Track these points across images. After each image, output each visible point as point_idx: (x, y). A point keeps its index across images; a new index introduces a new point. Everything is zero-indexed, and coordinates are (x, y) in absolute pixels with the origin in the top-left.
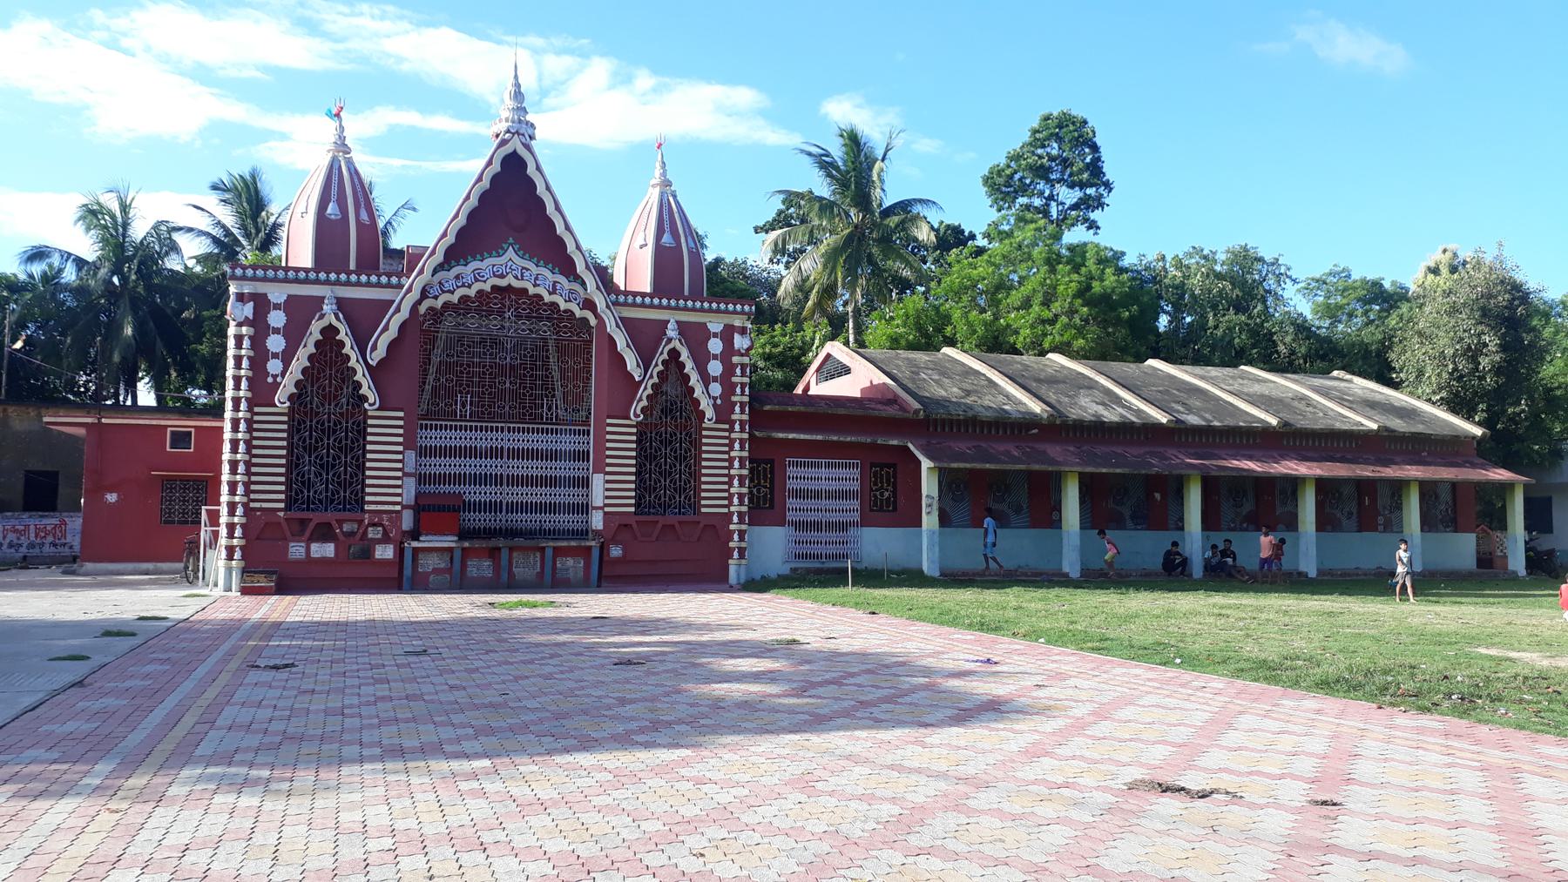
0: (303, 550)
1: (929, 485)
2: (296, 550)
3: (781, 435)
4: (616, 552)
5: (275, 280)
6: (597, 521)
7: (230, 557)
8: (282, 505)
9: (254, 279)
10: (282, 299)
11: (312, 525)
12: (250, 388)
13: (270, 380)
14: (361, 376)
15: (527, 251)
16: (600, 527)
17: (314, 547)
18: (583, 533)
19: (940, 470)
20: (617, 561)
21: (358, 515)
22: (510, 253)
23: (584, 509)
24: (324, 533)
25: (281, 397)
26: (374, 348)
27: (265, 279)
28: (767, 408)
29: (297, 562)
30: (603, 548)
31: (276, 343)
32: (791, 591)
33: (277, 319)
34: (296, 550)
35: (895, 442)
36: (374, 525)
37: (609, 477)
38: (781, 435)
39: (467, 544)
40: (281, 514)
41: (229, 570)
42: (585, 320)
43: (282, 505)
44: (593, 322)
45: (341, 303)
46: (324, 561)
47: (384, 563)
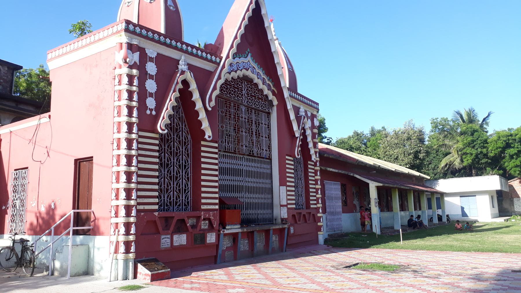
0: (169, 240)
1: (373, 194)
2: (165, 241)
3: (331, 170)
4: (292, 231)
5: (153, 40)
6: (284, 213)
7: (127, 251)
8: (156, 207)
9: (140, 35)
10: (154, 55)
11: (174, 221)
12: (139, 117)
13: (148, 112)
14: (202, 116)
15: (255, 59)
16: (285, 216)
17: (175, 237)
18: (271, 221)
19: (378, 188)
20: (294, 235)
21: (196, 213)
22: (249, 58)
23: (271, 206)
24: (181, 227)
25: (161, 125)
26: (210, 100)
27: (147, 38)
28: (325, 155)
29: (166, 250)
30: (289, 229)
31: (151, 86)
32: (382, 245)
33: (151, 68)
34: (165, 241)
35: (352, 175)
36: (204, 219)
37: (288, 188)
38: (331, 170)
39: (245, 230)
40: (156, 214)
41: (126, 261)
42: (271, 102)
43: (156, 207)
44: (275, 102)
45: (191, 67)
46: (181, 248)
47: (211, 245)
